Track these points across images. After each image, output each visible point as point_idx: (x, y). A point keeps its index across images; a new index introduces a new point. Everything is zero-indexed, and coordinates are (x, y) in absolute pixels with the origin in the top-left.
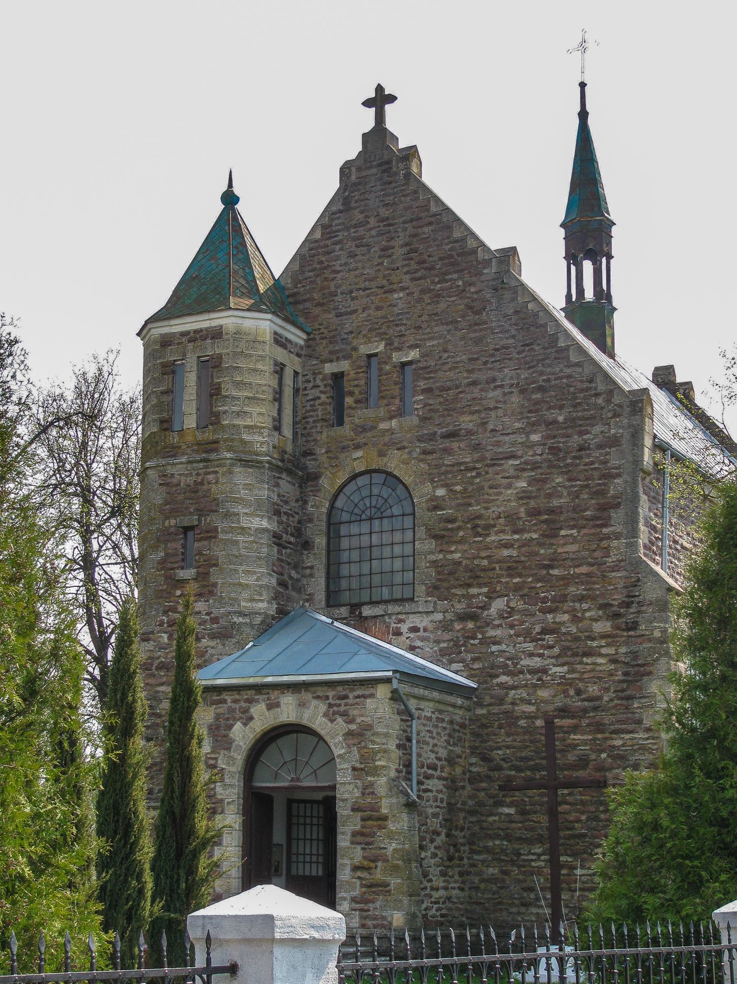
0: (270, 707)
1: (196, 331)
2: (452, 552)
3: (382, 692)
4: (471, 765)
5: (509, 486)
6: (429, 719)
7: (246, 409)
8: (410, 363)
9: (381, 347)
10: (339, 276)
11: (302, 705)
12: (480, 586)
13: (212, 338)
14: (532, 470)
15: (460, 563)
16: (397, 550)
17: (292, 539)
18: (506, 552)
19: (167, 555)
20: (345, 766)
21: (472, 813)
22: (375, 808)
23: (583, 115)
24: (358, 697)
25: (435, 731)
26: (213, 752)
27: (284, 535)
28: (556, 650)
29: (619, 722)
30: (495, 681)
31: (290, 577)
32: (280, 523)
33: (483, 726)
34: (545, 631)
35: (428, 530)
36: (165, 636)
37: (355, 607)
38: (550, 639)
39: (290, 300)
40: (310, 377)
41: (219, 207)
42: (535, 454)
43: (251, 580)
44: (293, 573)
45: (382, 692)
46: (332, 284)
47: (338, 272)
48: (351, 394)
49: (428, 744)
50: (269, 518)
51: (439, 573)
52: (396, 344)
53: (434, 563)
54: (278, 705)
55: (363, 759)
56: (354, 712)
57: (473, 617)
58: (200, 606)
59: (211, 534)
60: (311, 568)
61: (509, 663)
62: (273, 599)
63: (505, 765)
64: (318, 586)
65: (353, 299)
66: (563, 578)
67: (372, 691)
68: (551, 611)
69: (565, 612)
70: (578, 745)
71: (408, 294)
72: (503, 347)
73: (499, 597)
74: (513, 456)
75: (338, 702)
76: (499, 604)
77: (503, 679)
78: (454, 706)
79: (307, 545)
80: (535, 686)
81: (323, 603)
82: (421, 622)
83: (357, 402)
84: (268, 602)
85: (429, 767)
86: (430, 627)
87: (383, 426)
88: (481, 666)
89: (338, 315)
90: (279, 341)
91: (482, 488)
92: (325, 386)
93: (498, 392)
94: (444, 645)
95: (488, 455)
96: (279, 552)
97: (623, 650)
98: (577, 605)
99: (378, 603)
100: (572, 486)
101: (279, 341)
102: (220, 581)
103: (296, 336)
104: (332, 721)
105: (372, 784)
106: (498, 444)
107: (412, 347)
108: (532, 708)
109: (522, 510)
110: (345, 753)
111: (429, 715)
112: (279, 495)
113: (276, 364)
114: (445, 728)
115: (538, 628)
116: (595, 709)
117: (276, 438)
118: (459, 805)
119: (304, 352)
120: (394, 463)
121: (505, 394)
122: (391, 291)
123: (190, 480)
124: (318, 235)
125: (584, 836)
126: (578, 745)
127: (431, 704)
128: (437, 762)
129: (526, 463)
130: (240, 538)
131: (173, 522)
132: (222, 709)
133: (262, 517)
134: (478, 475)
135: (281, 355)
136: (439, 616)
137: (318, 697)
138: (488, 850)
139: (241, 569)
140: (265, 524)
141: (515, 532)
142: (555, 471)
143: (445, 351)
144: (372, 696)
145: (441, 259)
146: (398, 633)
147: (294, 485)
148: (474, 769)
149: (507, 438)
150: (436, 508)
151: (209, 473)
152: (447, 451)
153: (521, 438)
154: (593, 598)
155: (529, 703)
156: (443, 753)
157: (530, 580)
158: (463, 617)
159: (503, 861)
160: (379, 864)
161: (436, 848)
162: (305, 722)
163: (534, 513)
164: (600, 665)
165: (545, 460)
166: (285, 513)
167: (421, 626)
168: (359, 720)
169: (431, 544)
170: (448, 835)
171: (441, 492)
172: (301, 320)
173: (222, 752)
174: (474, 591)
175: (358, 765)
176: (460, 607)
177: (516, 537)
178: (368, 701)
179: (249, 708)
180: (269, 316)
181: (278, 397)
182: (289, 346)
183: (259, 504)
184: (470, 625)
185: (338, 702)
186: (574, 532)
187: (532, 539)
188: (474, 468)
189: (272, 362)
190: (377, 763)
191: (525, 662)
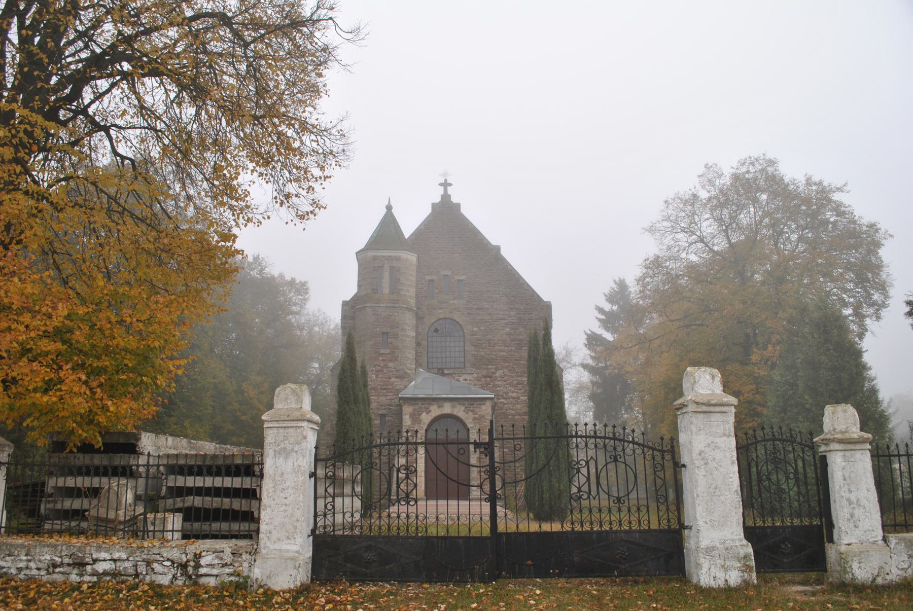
0: (439, 407)
3: (489, 404)
5: (503, 330)
9: (449, 273)
11: (453, 407)
12: (492, 365)
16: (457, 349)
18: (502, 354)
28: (523, 391)
38: (520, 386)
41: (384, 211)
45: (489, 404)
57: (490, 377)
58: (390, 364)
68: (520, 376)
74: (505, 319)
76: (499, 373)
77: (502, 400)
82: (469, 377)
86: (472, 379)
87: (452, 302)
108: (514, 412)
115: (515, 382)
132: (416, 407)
136: (475, 375)
144: (484, 404)
150: (474, 335)
153: (507, 313)
155: (513, 410)
158: (485, 377)
162: (455, 413)
167: (468, 379)
171: (475, 329)
174: (490, 367)
176: (484, 372)
184: (488, 379)
191: (510, 394)
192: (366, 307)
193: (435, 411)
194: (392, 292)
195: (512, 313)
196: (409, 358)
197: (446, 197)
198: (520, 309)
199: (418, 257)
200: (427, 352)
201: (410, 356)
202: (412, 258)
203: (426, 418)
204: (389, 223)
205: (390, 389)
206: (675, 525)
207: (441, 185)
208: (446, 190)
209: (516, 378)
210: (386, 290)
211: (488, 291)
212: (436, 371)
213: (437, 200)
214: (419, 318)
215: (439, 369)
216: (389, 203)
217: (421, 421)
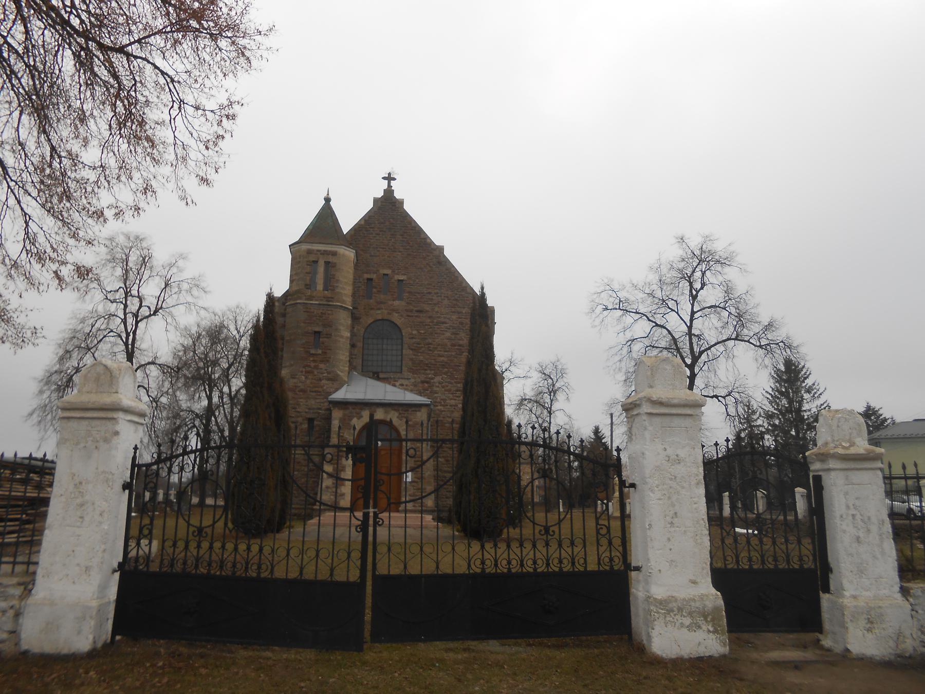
1: (324, 251)
5: (444, 334)
7: (345, 287)
8: (402, 281)
10: (372, 241)
11: (386, 412)
12: (431, 370)
13: (332, 255)
15: (422, 361)
18: (442, 359)
24: (413, 411)
42: (453, 323)
48: (376, 288)
53: (412, 360)
57: (427, 382)
58: (322, 366)
59: (329, 336)
60: (356, 355)
65: (378, 251)
72: (441, 282)
74: (446, 323)
76: (438, 379)
80: (453, 411)
82: (405, 382)
95: (435, 321)
99: (385, 372)
104: (401, 420)
106: (439, 317)
107: (405, 274)
124: (363, 222)
129: (450, 326)
130: (341, 340)
131: (310, 328)
134: (431, 328)
136: (413, 380)
139: (341, 352)
141: (445, 352)
144: (419, 411)
149: (442, 316)
150: (413, 338)
158: (423, 382)
167: (405, 384)
171: (415, 332)
174: (428, 372)
176: (423, 377)
178: (418, 413)
187: (452, 355)
192: (297, 303)
194: (326, 288)
197: (389, 192)
198: (461, 313)
199: (356, 252)
200: (363, 355)
201: (341, 357)
202: (349, 254)
204: (326, 217)
205: (320, 392)
206: (618, 565)
207: (384, 178)
208: (389, 186)
209: (455, 384)
210: (320, 287)
211: (430, 293)
212: (371, 374)
213: (380, 194)
214: (355, 318)
215: (374, 373)
216: (328, 194)
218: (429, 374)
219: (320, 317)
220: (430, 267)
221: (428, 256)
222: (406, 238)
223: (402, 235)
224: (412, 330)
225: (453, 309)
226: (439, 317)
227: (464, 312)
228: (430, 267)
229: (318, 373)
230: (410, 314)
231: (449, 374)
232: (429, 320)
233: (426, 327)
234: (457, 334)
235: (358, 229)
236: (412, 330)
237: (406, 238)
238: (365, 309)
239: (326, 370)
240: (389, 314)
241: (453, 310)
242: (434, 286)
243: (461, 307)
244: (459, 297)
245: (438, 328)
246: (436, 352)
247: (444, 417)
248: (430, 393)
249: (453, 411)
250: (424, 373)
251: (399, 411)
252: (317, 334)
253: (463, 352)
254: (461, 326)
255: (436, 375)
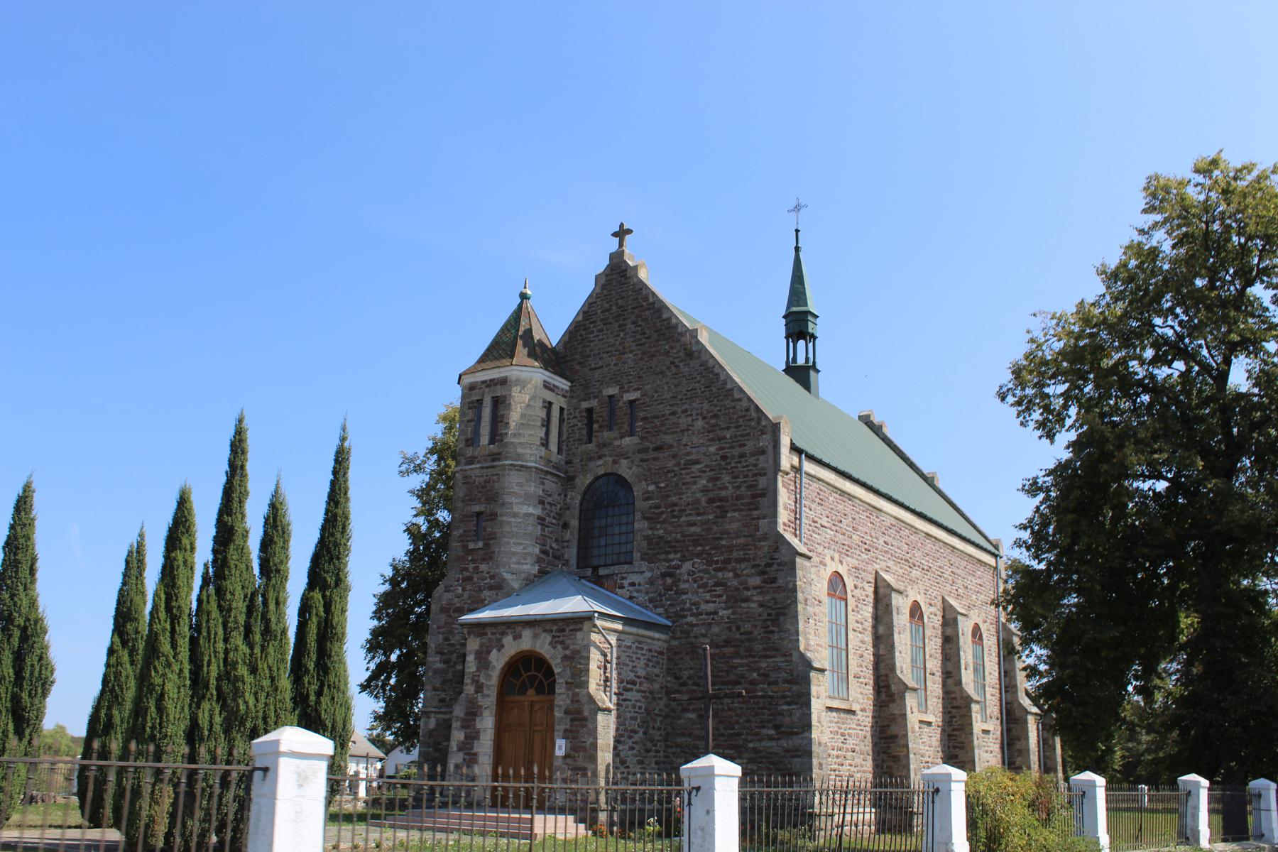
1: (491, 380)
2: (658, 529)
4: (667, 681)
5: (695, 483)
6: (630, 647)
7: (521, 431)
8: (634, 401)
10: (592, 344)
11: (536, 636)
12: (675, 552)
13: (501, 384)
14: (710, 471)
15: (662, 537)
17: (554, 521)
18: (693, 529)
19: (465, 531)
20: (561, 681)
21: (667, 716)
22: (579, 712)
23: (797, 249)
24: (572, 630)
25: (634, 656)
26: (477, 670)
27: (547, 518)
28: (724, 597)
29: (765, 649)
30: (685, 620)
31: (551, 547)
32: (544, 509)
33: (676, 653)
34: (717, 584)
35: (643, 514)
36: (460, 588)
37: (595, 569)
38: (719, 590)
39: (562, 360)
40: (571, 411)
43: (519, 549)
44: (554, 545)
46: (588, 349)
47: (592, 341)
49: (628, 665)
50: (535, 506)
51: (648, 544)
52: (626, 388)
53: (647, 538)
54: (520, 636)
55: (573, 676)
56: (568, 642)
57: (671, 575)
58: (483, 567)
59: (493, 516)
60: (568, 541)
61: (694, 607)
62: (535, 562)
63: (690, 682)
64: (572, 553)
65: (601, 359)
66: (729, 547)
67: (579, 626)
69: (730, 571)
70: (737, 667)
71: (635, 355)
72: (693, 389)
73: (688, 560)
74: (697, 462)
75: (558, 634)
76: (687, 566)
78: (653, 639)
79: (565, 526)
80: (710, 624)
81: (575, 566)
83: (600, 427)
84: (531, 565)
85: (628, 683)
87: (617, 443)
88: (674, 610)
89: (591, 369)
90: (547, 386)
91: (677, 485)
92: (581, 417)
93: (689, 419)
94: (652, 595)
95: (682, 462)
96: (543, 530)
97: (768, 597)
98: (738, 566)
100: (735, 482)
101: (547, 386)
102: (497, 550)
103: (563, 384)
104: (554, 648)
105: (578, 694)
106: (689, 454)
109: (703, 499)
110: (562, 672)
111: (629, 644)
112: (543, 490)
113: (544, 401)
114: (643, 655)
115: (711, 582)
116: (749, 640)
117: (543, 451)
118: (656, 712)
119: (568, 395)
120: (626, 470)
121: (693, 420)
122: (624, 354)
123: (482, 480)
124: (580, 318)
125: (740, 734)
126: (737, 667)
127: (631, 637)
128: (636, 679)
130: (513, 520)
133: (529, 505)
134: (675, 475)
135: (549, 396)
136: (648, 574)
137: (545, 631)
138: (678, 746)
139: (512, 541)
140: (531, 510)
141: (698, 514)
142: (724, 471)
143: (657, 392)
144: (581, 629)
145: (655, 332)
146: (622, 587)
147: (557, 483)
148: (669, 685)
149: (694, 450)
151: (493, 475)
152: (656, 459)
154: (748, 560)
156: (642, 673)
157: (707, 548)
158: (664, 575)
159: (687, 753)
160: (581, 754)
161: (633, 743)
163: (711, 501)
164: (753, 608)
165: (719, 464)
166: (549, 503)
167: (637, 582)
168: (572, 647)
169: (646, 524)
170: (645, 733)
171: (651, 488)
172: (568, 373)
173: (483, 671)
174: (672, 556)
175: (570, 680)
176: (663, 567)
177: (699, 518)
178: (578, 633)
179: (502, 639)
180: (540, 370)
181: (547, 423)
182: (556, 390)
183: (528, 497)
184: (669, 581)
185: (558, 634)
186: (736, 514)
188: (673, 471)
189: (541, 401)
190: (582, 679)
191: (703, 607)
193: (511, 647)
194: (492, 442)
195: (712, 449)
196: (514, 554)
203: (499, 660)
207: (615, 235)
210: (484, 440)
213: (602, 264)
217: (490, 663)
218: (672, 560)
219: (483, 487)
220: (676, 366)
221: (672, 348)
222: (640, 326)
223: (634, 323)
224: (648, 485)
225: (711, 435)
226: (689, 454)
227: (728, 436)
228: (676, 366)
229: (478, 579)
230: (644, 456)
231: (704, 556)
232: (673, 462)
233: (669, 475)
234: (717, 479)
235: (577, 331)
236: (648, 485)
237: (640, 326)
238: (581, 461)
239: (488, 573)
240: (615, 462)
241: (711, 435)
242: (681, 400)
243: (723, 429)
244: (720, 410)
245: (687, 474)
246: (683, 519)
247: (696, 637)
248: (675, 593)
249: (710, 624)
250: (665, 560)
251: (552, 631)
252: (479, 514)
253: (727, 512)
254: (723, 463)
255: (683, 559)
